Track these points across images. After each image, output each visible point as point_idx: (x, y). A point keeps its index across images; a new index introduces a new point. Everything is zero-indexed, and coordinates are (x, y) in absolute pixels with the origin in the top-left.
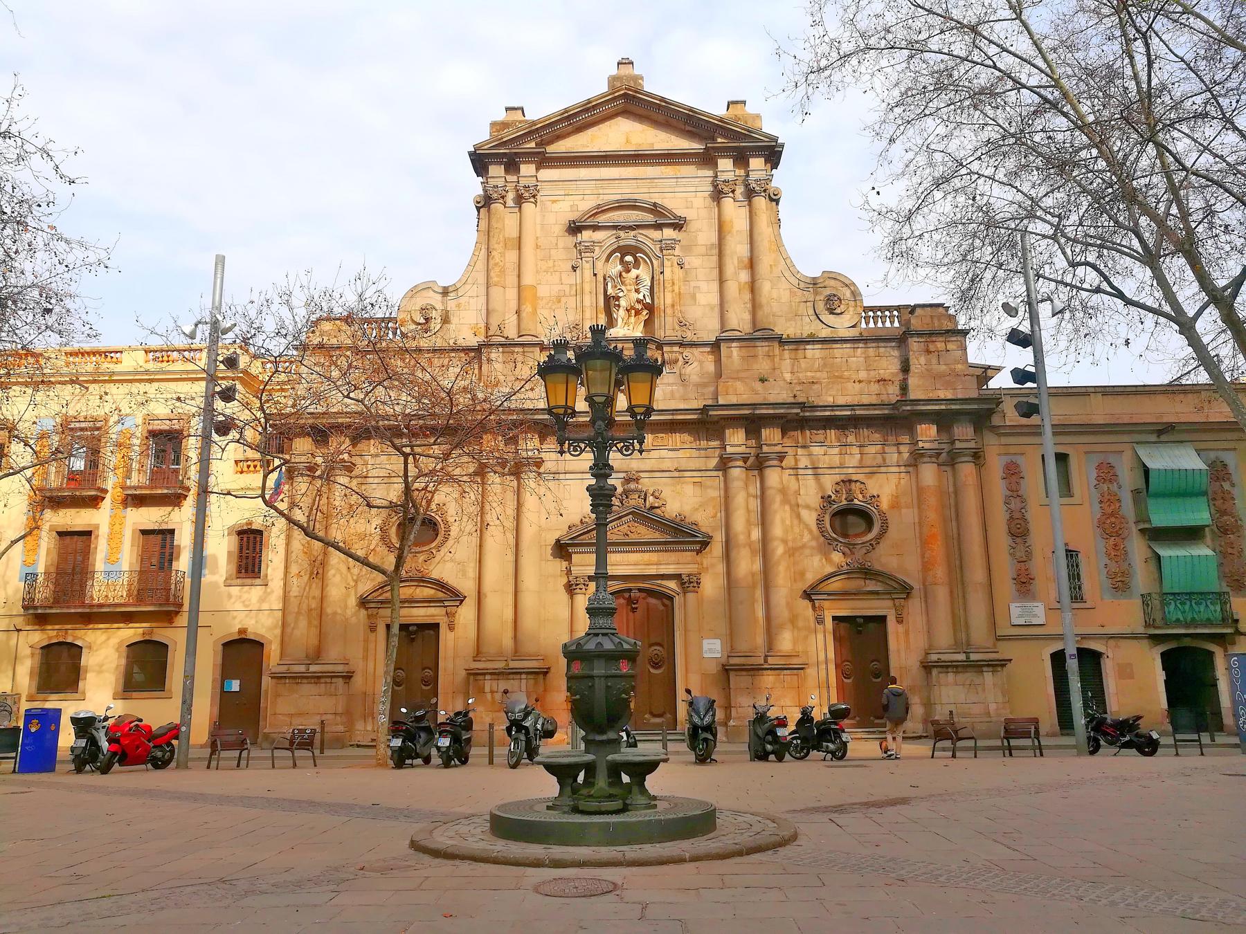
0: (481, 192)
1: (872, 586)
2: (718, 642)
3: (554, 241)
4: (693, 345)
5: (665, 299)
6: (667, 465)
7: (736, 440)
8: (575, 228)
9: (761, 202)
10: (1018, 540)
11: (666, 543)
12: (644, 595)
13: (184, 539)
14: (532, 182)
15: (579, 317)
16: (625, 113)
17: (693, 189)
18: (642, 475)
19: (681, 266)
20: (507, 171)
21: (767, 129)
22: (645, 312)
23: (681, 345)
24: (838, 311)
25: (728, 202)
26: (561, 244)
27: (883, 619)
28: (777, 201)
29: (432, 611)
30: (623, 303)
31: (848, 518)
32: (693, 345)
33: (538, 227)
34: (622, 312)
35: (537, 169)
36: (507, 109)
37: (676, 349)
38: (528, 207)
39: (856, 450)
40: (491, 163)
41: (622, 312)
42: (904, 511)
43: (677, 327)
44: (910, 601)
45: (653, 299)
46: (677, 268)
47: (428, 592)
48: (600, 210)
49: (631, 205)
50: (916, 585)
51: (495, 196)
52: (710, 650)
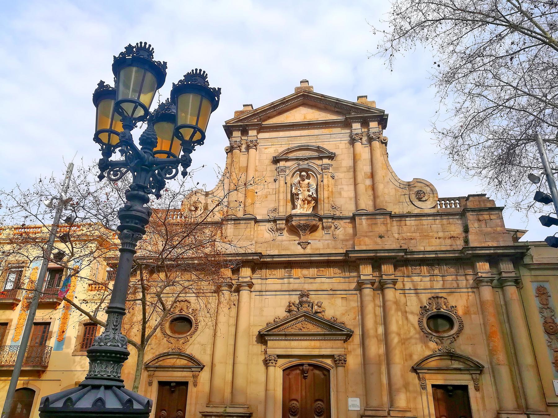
2: (358, 400)
3: (265, 167)
4: (340, 218)
5: (324, 195)
6: (325, 287)
7: (367, 271)
8: (276, 161)
9: (376, 144)
10: (552, 337)
11: (324, 335)
12: (311, 368)
13: (55, 328)
15: (277, 205)
16: (304, 104)
17: (339, 139)
18: (311, 293)
20: (243, 134)
22: (313, 202)
23: (333, 218)
24: (424, 199)
25: (358, 145)
28: (386, 144)
29: (185, 374)
30: (300, 196)
31: (438, 320)
32: (340, 218)
33: (257, 161)
34: (300, 201)
35: (258, 133)
36: (244, 106)
37: (330, 220)
38: (252, 151)
39: (440, 278)
41: (300, 201)
42: (473, 316)
43: (331, 209)
44: (483, 376)
45: (317, 195)
46: (331, 179)
47: (183, 362)
48: (289, 151)
50: (486, 365)
51: (235, 146)
52: (353, 405)
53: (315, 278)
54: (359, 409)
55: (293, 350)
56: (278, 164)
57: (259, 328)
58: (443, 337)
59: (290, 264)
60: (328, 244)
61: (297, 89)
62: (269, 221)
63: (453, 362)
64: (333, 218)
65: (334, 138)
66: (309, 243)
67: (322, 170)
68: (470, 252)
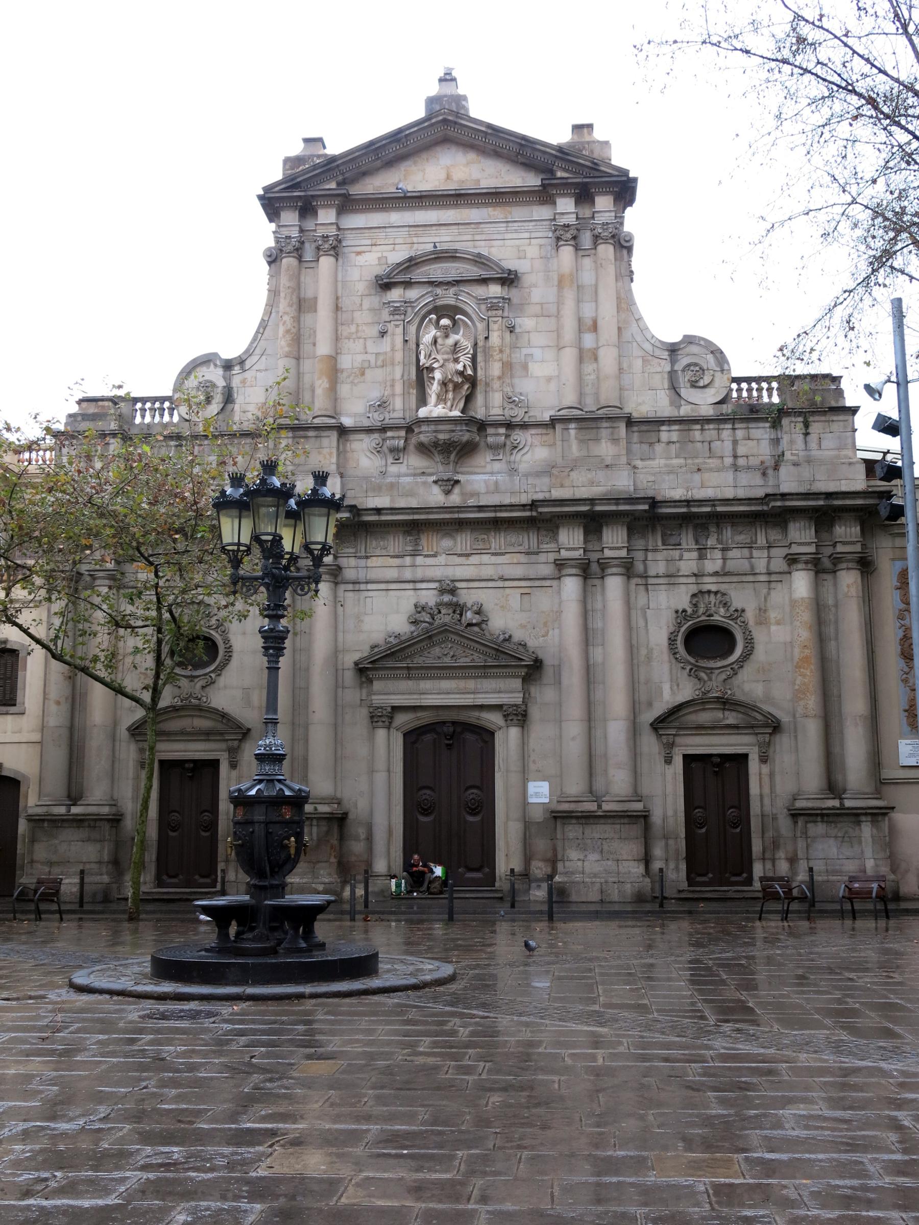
0: (273, 244)
1: (731, 718)
4: (524, 426)
6: (488, 572)
7: (571, 540)
8: (385, 284)
14: (333, 231)
16: (445, 141)
17: (527, 235)
18: (458, 585)
19: (512, 329)
21: (618, 159)
24: (701, 384)
26: (366, 303)
27: (743, 758)
28: (629, 249)
30: (438, 375)
31: (707, 639)
36: (307, 141)
37: (502, 431)
39: (718, 554)
40: (283, 208)
42: (773, 628)
44: (777, 738)
45: (475, 369)
48: (412, 263)
49: (451, 256)
50: (785, 719)
52: (537, 794)
53: (468, 555)
54: (547, 801)
55: (422, 696)
56: (388, 293)
57: (357, 656)
58: (712, 669)
59: (416, 526)
60: (496, 483)
61: (430, 101)
62: (369, 431)
63: (727, 713)
64: (509, 426)
65: (516, 231)
66: (457, 482)
68: (779, 504)
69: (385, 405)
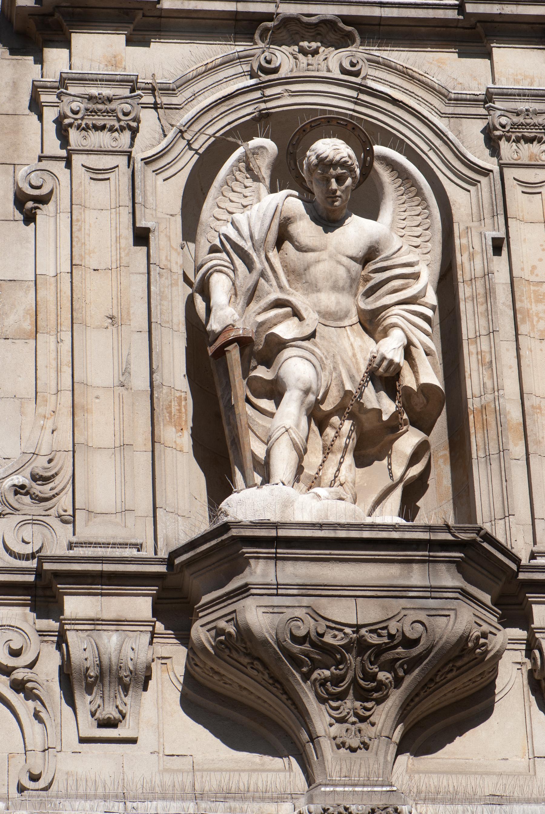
30: (296, 368)
34: (290, 412)
41: (290, 412)
67: (492, 142)
69: (45, 490)
